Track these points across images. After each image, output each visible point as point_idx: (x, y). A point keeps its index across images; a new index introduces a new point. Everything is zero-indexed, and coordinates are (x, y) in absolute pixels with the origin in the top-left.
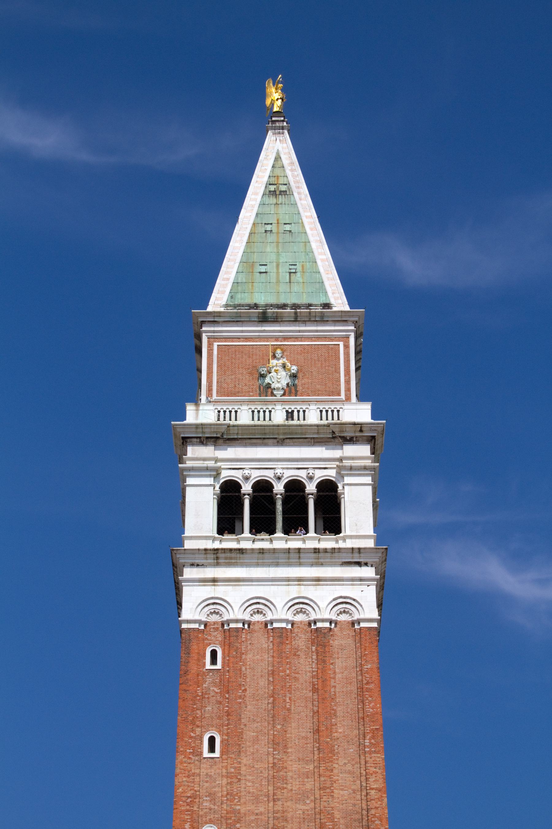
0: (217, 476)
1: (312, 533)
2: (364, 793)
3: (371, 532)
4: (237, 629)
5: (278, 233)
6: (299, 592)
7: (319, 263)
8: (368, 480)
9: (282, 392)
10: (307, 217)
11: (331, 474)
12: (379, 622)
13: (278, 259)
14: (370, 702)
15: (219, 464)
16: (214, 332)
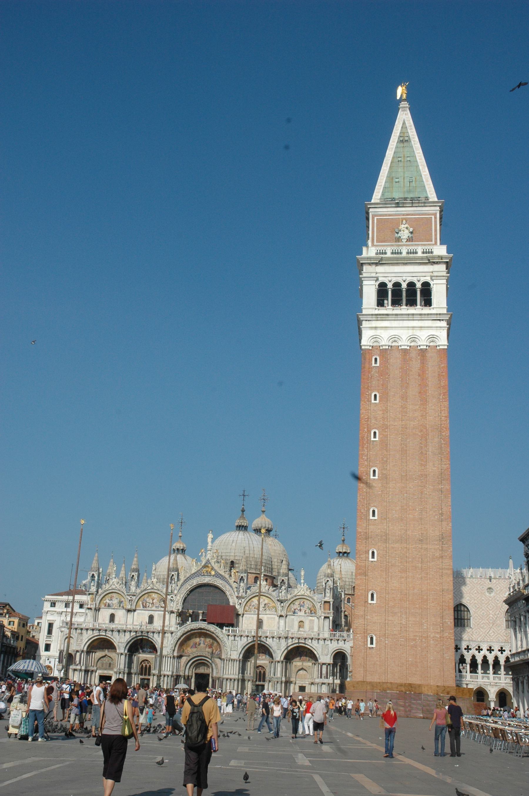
0: (377, 280)
1: (418, 306)
2: (439, 418)
3: (445, 306)
4: (386, 349)
5: (404, 162)
6: (413, 333)
7: (423, 176)
8: (444, 281)
9: (406, 240)
10: (418, 153)
11: (428, 279)
12: (448, 346)
13: (404, 175)
14: (443, 381)
15: (378, 275)
16: (375, 212)
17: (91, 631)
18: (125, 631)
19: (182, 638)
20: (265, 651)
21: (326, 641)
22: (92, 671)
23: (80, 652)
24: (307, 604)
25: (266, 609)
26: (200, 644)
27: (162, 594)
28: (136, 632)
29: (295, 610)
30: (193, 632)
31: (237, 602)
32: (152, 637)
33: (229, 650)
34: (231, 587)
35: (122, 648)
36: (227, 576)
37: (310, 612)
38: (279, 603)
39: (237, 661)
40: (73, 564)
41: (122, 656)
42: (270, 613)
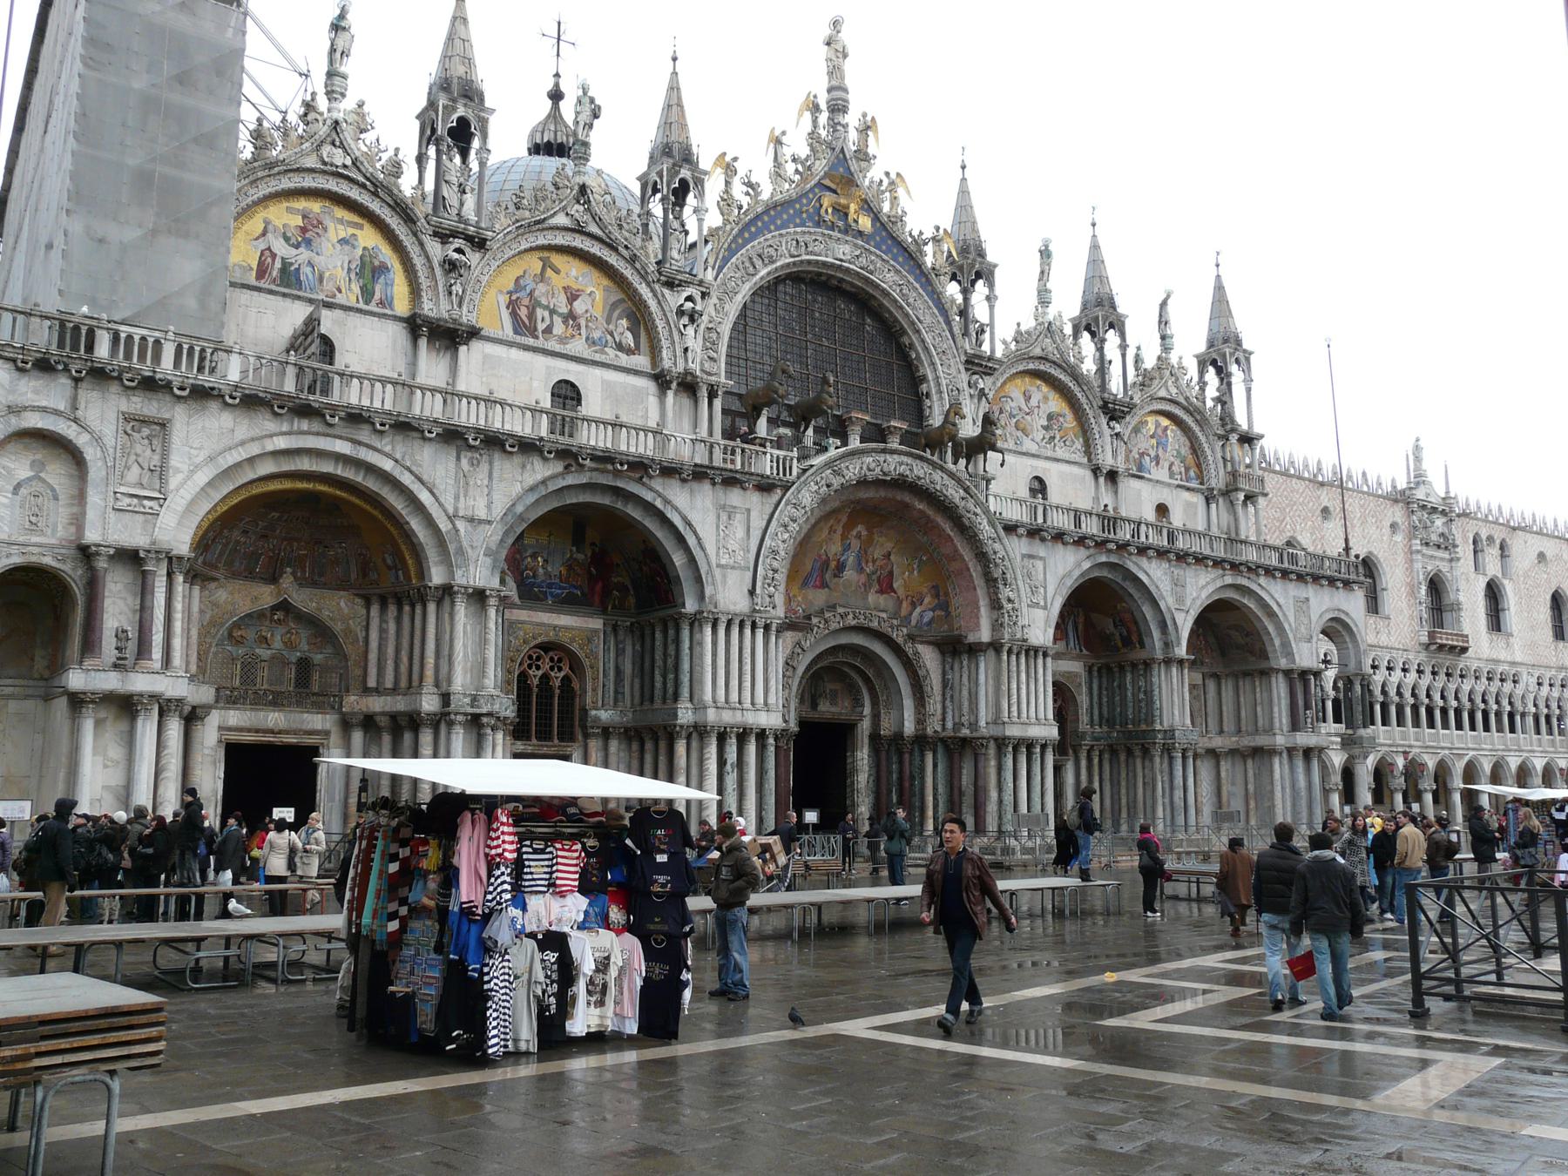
25: (1054, 438)
26: (841, 567)
27: (628, 272)
38: (1103, 420)
39: (1045, 655)
42: (1067, 456)
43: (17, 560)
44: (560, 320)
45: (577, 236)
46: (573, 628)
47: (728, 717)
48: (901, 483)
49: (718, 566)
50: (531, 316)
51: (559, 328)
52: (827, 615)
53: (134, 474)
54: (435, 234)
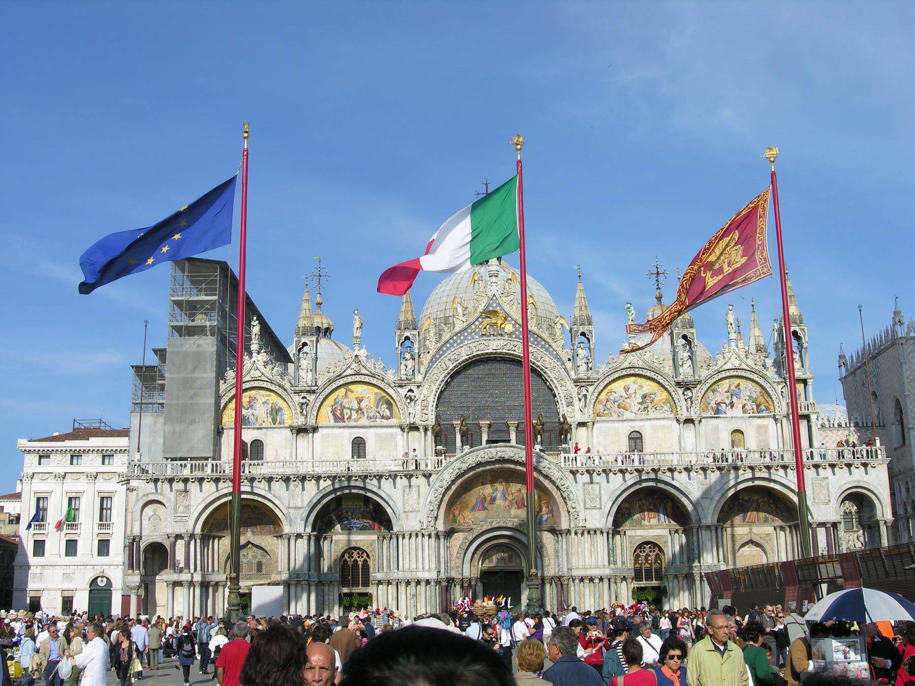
17: (213, 485)
18: (303, 479)
19: (454, 488)
20: (655, 506)
21: (820, 470)
22: (217, 584)
23: (186, 539)
24: (748, 389)
26: (493, 500)
27: (382, 385)
28: (334, 478)
29: (718, 404)
30: (481, 469)
31: (574, 394)
32: (375, 490)
33: (580, 507)
34: (558, 357)
35: (299, 520)
36: (546, 336)
37: (755, 407)
38: (680, 391)
39: (602, 533)
40: (146, 322)
41: (299, 541)
43: (151, 541)
44: (355, 412)
45: (357, 376)
46: (363, 540)
47: (409, 576)
48: (503, 461)
49: (404, 512)
50: (342, 413)
51: (354, 415)
52: (481, 523)
53: (181, 509)
54: (295, 393)
